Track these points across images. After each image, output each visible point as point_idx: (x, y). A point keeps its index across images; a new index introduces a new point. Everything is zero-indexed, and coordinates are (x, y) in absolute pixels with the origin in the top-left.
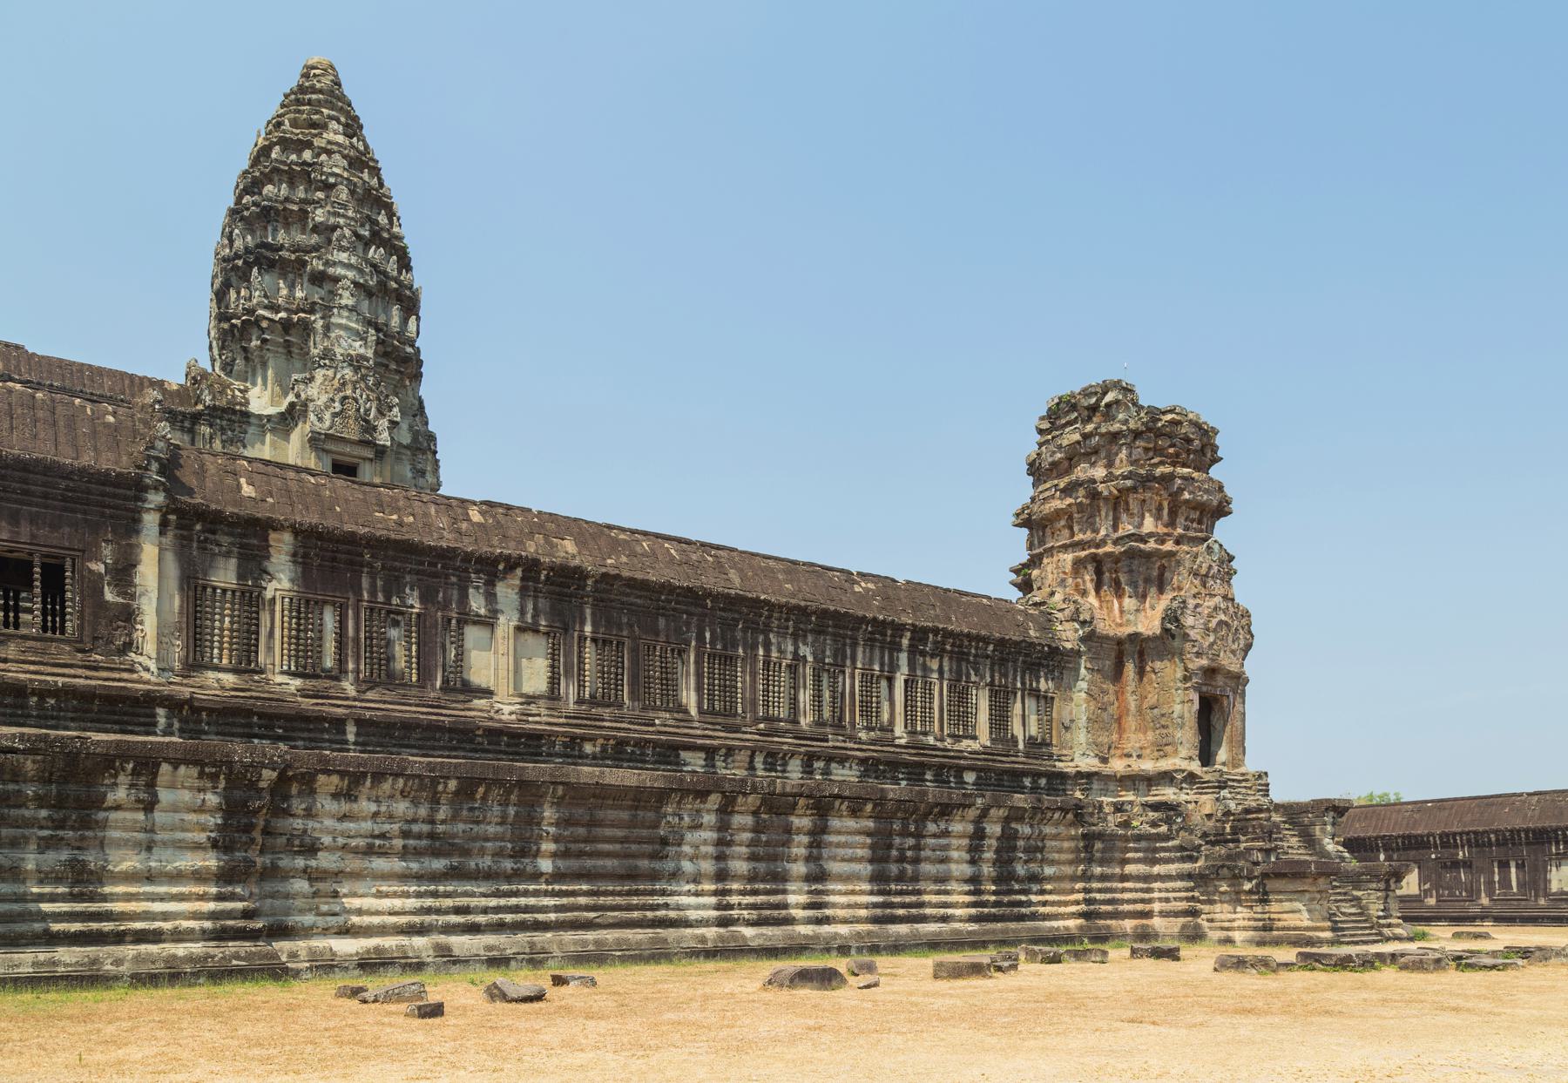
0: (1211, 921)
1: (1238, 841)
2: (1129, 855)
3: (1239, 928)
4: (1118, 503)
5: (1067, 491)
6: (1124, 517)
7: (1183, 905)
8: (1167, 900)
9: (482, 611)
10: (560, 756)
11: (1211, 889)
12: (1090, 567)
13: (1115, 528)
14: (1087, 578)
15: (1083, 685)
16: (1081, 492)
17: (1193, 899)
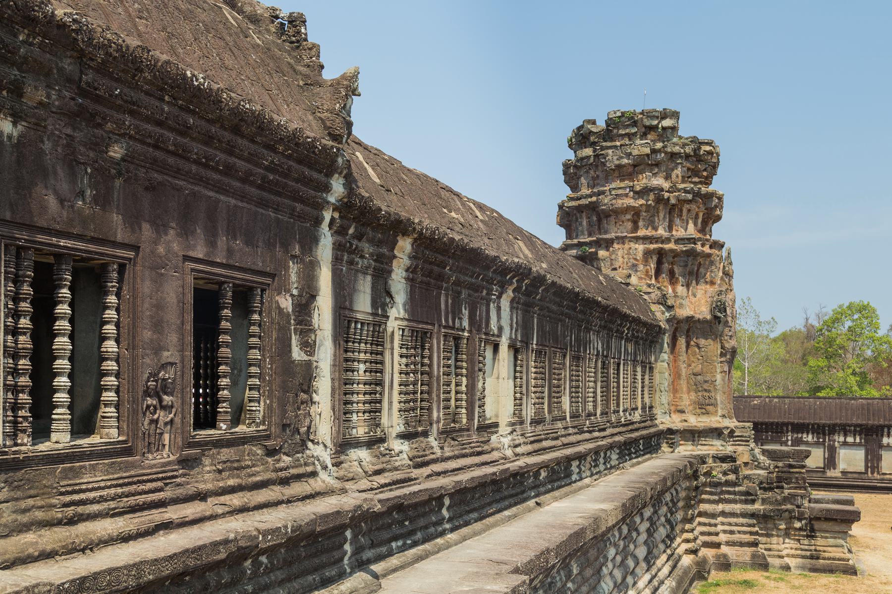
0: (770, 550)
1: (782, 488)
2: (704, 496)
3: (788, 555)
4: (674, 211)
6: (677, 221)
7: (747, 538)
8: (732, 532)
9: (496, 332)
11: (770, 526)
12: (655, 258)
13: (670, 228)
14: (652, 266)
15: (665, 356)
16: (652, 196)
17: (756, 533)
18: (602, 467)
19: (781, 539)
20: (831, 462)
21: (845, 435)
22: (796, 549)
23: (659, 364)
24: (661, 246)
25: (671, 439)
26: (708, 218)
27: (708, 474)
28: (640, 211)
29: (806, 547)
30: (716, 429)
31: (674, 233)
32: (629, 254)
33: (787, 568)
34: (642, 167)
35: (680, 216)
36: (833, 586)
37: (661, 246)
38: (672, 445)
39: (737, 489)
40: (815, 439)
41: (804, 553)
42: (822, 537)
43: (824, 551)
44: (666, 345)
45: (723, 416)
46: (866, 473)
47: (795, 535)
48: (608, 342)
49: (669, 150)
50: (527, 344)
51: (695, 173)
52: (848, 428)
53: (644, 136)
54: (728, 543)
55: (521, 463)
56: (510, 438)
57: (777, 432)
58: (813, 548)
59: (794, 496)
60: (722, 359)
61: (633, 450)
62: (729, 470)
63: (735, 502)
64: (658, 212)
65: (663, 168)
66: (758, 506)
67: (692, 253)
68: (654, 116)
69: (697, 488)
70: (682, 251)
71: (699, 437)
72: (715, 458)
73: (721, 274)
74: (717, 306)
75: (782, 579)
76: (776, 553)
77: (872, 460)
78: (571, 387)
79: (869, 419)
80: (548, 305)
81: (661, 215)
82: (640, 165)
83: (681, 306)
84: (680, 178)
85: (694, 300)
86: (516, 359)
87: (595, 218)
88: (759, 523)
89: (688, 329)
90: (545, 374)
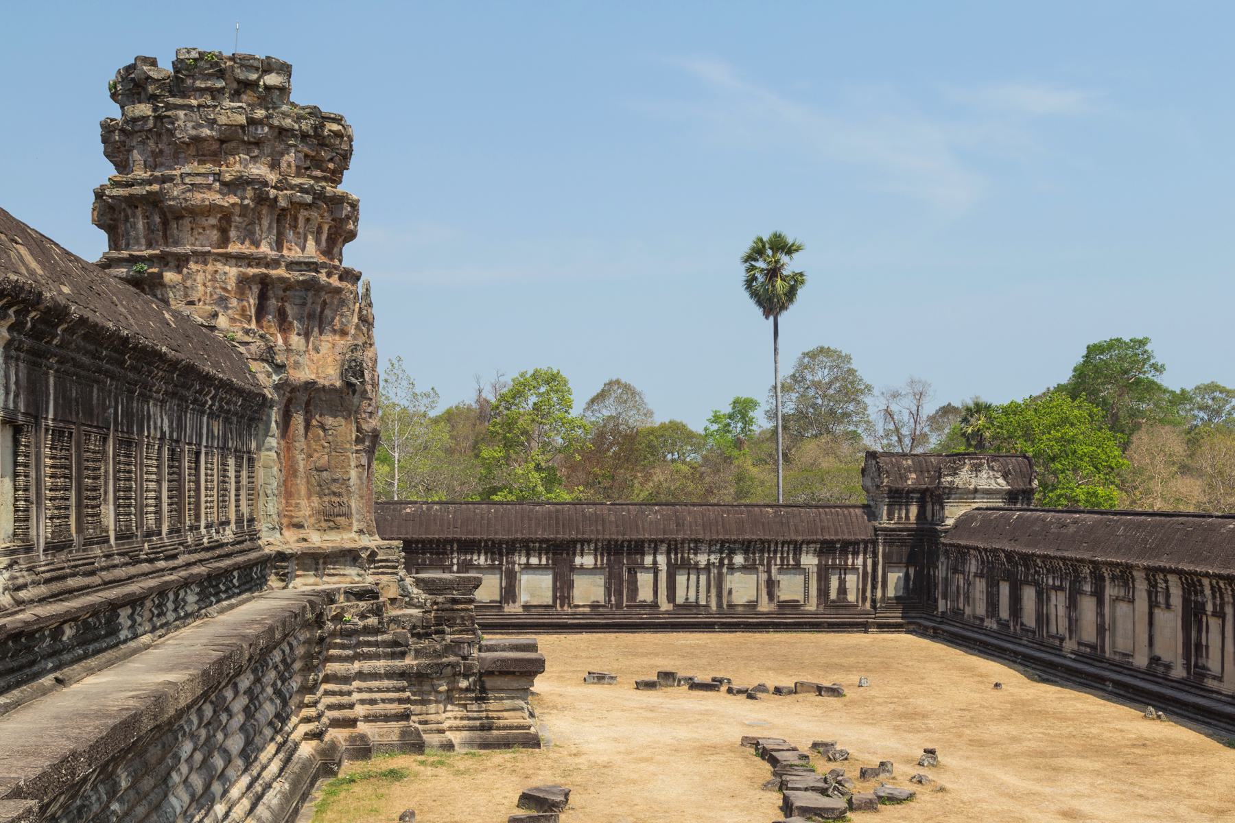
0: (426, 722)
1: (443, 632)
2: (332, 652)
3: (451, 729)
4: (285, 218)
5: (232, 186)
6: (290, 234)
7: (394, 708)
8: (373, 702)
10: (51, 655)
11: (426, 688)
12: (256, 289)
13: (279, 245)
14: (252, 301)
15: (273, 442)
16: (249, 193)
17: (408, 700)
18: (171, 616)
19: (441, 706)
20: (509, 593)
21: (528, 556)
22: (462, 718)
23: (263, 453)
24: (264, 271)
25: (283, 568)
26: (336, 233)
27: (338, 618)
28: (232, 214)
29: (475, 715)
30: (350, 551)
31: (285, 252)
32: (214, 280)
33: (449, 746)
34: (233, 144)
35: (294, 227)
36: (509, 765)
37: (264, 271)
38: (284, 577)
39: (380, 638)
40: (489, 562)
41: (471, 723)
42: (496, 699)
43: (499, 718)
44: (273, 425)
45: (361, 532)
46: (554, 606)
47: (460, 699)
48: (179, 419)
49: (276, 123)
50: (36, 418)
51: (317, 163)
52: (531, 545)
53: (236, 95)
54: (368, 719)
55: (27, 615)
56: (6, 575)
57: (438, 554)
58: (484, 714)
59: (457, 644)
60: (359, 447)
61: (222, 588)
62: (369, 611)
63: (377, 657)
64: (260, 219)
65: (267, 150)
66: (409, 661)
67: (311, 286)
68: (252, 66)
69: (322, 640)
70: (298, 282)
71: (325, 563)
72: (349, 594)
73: (356, 320)
74: (350, 367)
75: (442, 763)
76: (434, 726)
77: (562, 588)
78: (116, 490)
79: (558, 532)
80: (74, 355)
81: (265, 223)
82: (230, 141)
83: (297, 365)
84: (294, 168)
85: (315, 357)
86: (16, 443)
87: (157, 220)
88: (411, 685)
89: (307, 400)
90: (70, 468)
